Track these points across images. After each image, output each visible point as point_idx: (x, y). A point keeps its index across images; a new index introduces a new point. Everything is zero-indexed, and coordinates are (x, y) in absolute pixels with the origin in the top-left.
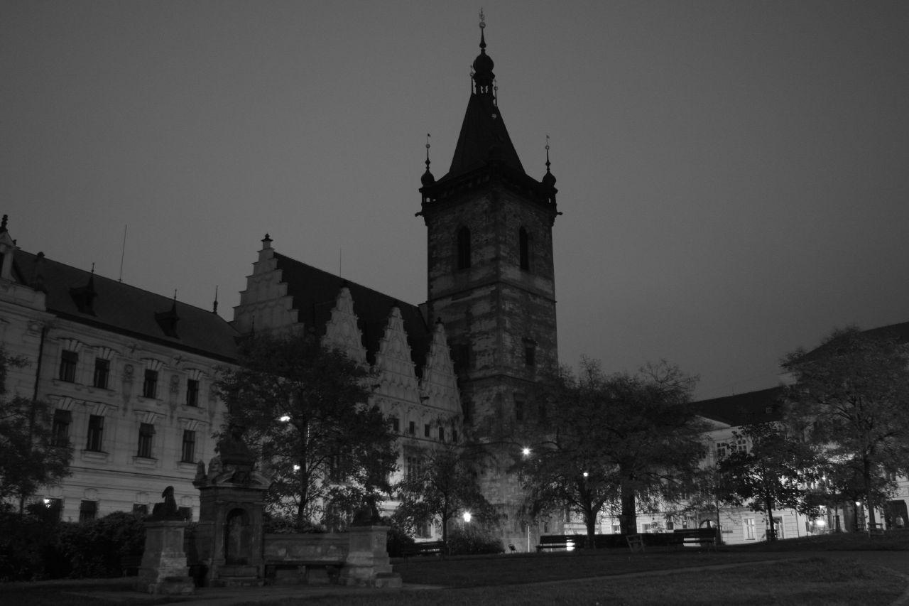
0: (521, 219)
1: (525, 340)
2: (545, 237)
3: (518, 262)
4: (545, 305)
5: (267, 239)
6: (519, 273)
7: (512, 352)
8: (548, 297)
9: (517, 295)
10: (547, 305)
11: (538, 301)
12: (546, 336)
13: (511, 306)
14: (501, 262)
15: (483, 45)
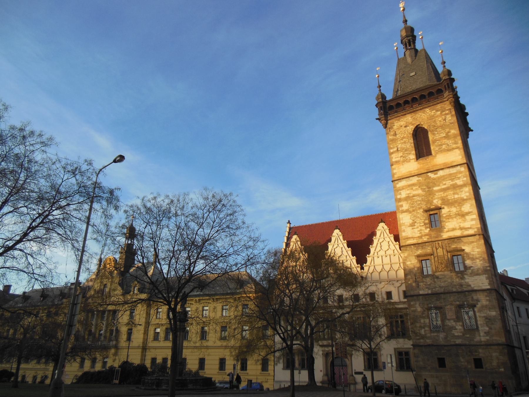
0: (413, 125)
1: (426, 211)
2: (445, 120)
3: (413, 156)
4: (452, 172)
5: (289, 222)
6: (416, 163)
7: (412, 225)
8: (455, 164)
9: (415, 180)
10: (453, 171)
11: (441, 173)
12: (456, 196)
13: (408, 192)
14: (393, 167)
15: (405, 21)
